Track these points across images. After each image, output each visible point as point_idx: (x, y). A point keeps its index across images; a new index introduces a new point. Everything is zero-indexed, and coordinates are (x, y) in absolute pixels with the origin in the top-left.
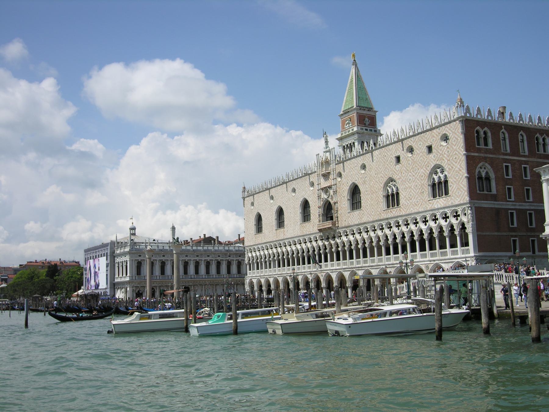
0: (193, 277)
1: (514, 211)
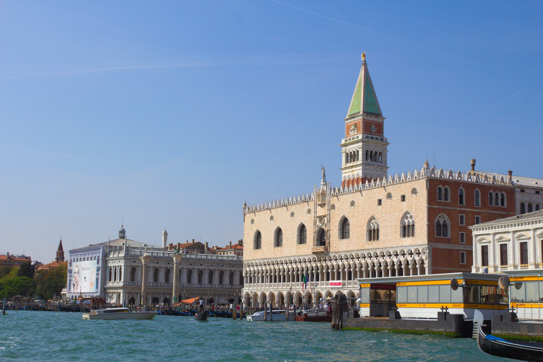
0: (185, 285)
1: (465, 252)
